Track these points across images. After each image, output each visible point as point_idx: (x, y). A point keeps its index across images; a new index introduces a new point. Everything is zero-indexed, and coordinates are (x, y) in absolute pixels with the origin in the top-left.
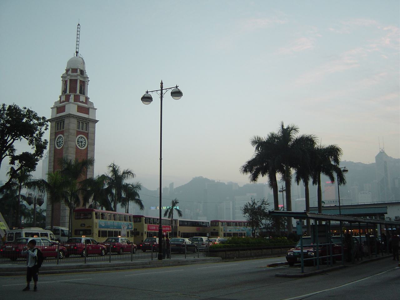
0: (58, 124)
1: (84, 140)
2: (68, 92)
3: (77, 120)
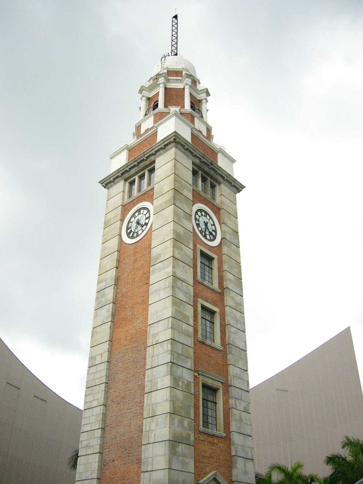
0: (132, 183)
1: (212, 223)
3: (194, 163)
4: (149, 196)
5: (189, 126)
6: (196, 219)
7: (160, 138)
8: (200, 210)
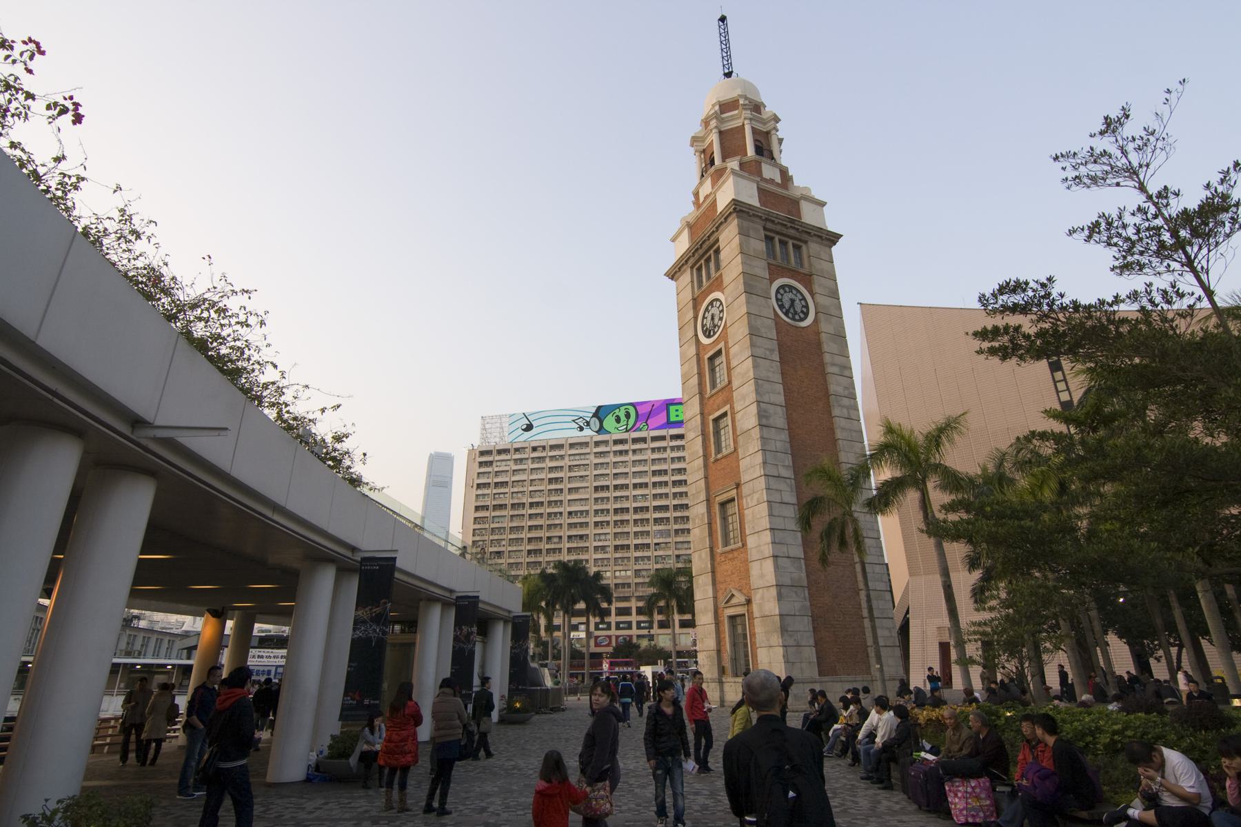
0: (699, 269)
2: (718, 161)
3: (765, 229)
4: (718, 285)
5: (753, 181)
6: (777, 300)
7: (720, 209)
8: (782, 287)
